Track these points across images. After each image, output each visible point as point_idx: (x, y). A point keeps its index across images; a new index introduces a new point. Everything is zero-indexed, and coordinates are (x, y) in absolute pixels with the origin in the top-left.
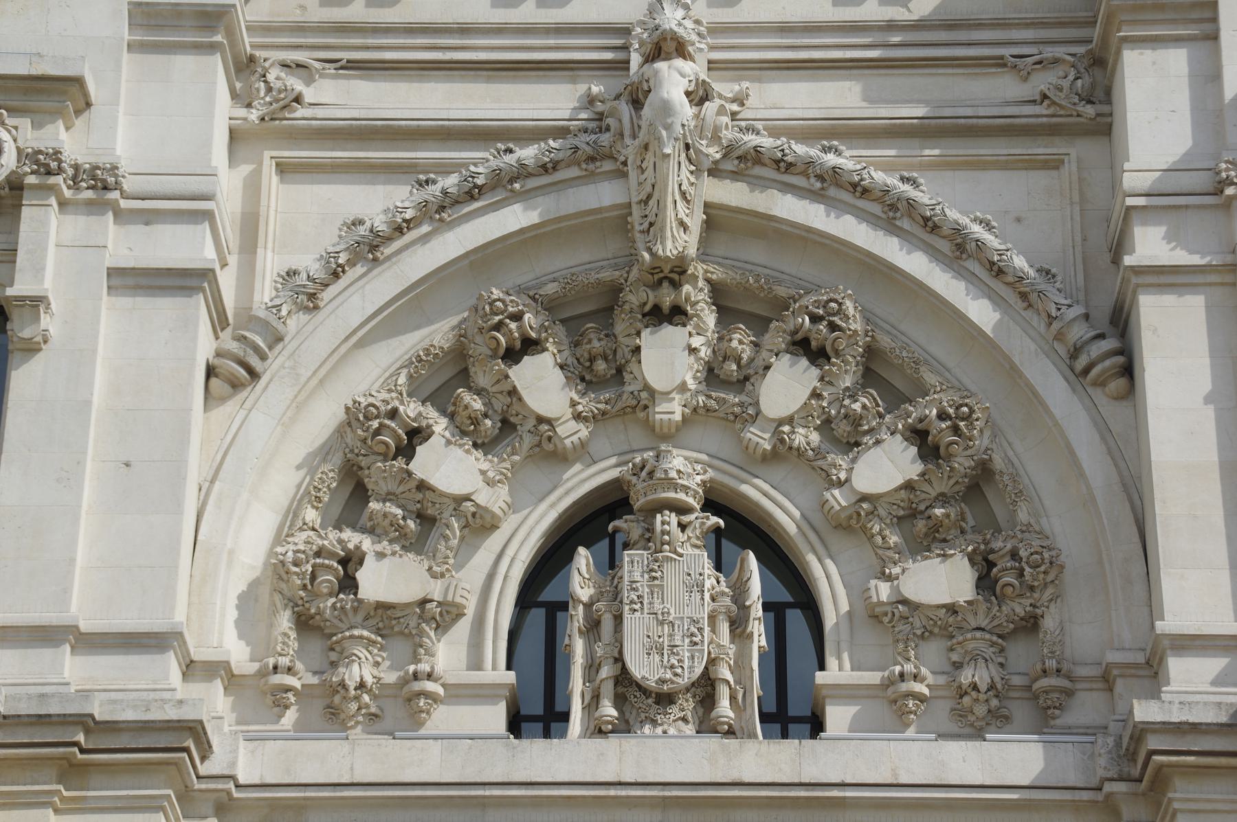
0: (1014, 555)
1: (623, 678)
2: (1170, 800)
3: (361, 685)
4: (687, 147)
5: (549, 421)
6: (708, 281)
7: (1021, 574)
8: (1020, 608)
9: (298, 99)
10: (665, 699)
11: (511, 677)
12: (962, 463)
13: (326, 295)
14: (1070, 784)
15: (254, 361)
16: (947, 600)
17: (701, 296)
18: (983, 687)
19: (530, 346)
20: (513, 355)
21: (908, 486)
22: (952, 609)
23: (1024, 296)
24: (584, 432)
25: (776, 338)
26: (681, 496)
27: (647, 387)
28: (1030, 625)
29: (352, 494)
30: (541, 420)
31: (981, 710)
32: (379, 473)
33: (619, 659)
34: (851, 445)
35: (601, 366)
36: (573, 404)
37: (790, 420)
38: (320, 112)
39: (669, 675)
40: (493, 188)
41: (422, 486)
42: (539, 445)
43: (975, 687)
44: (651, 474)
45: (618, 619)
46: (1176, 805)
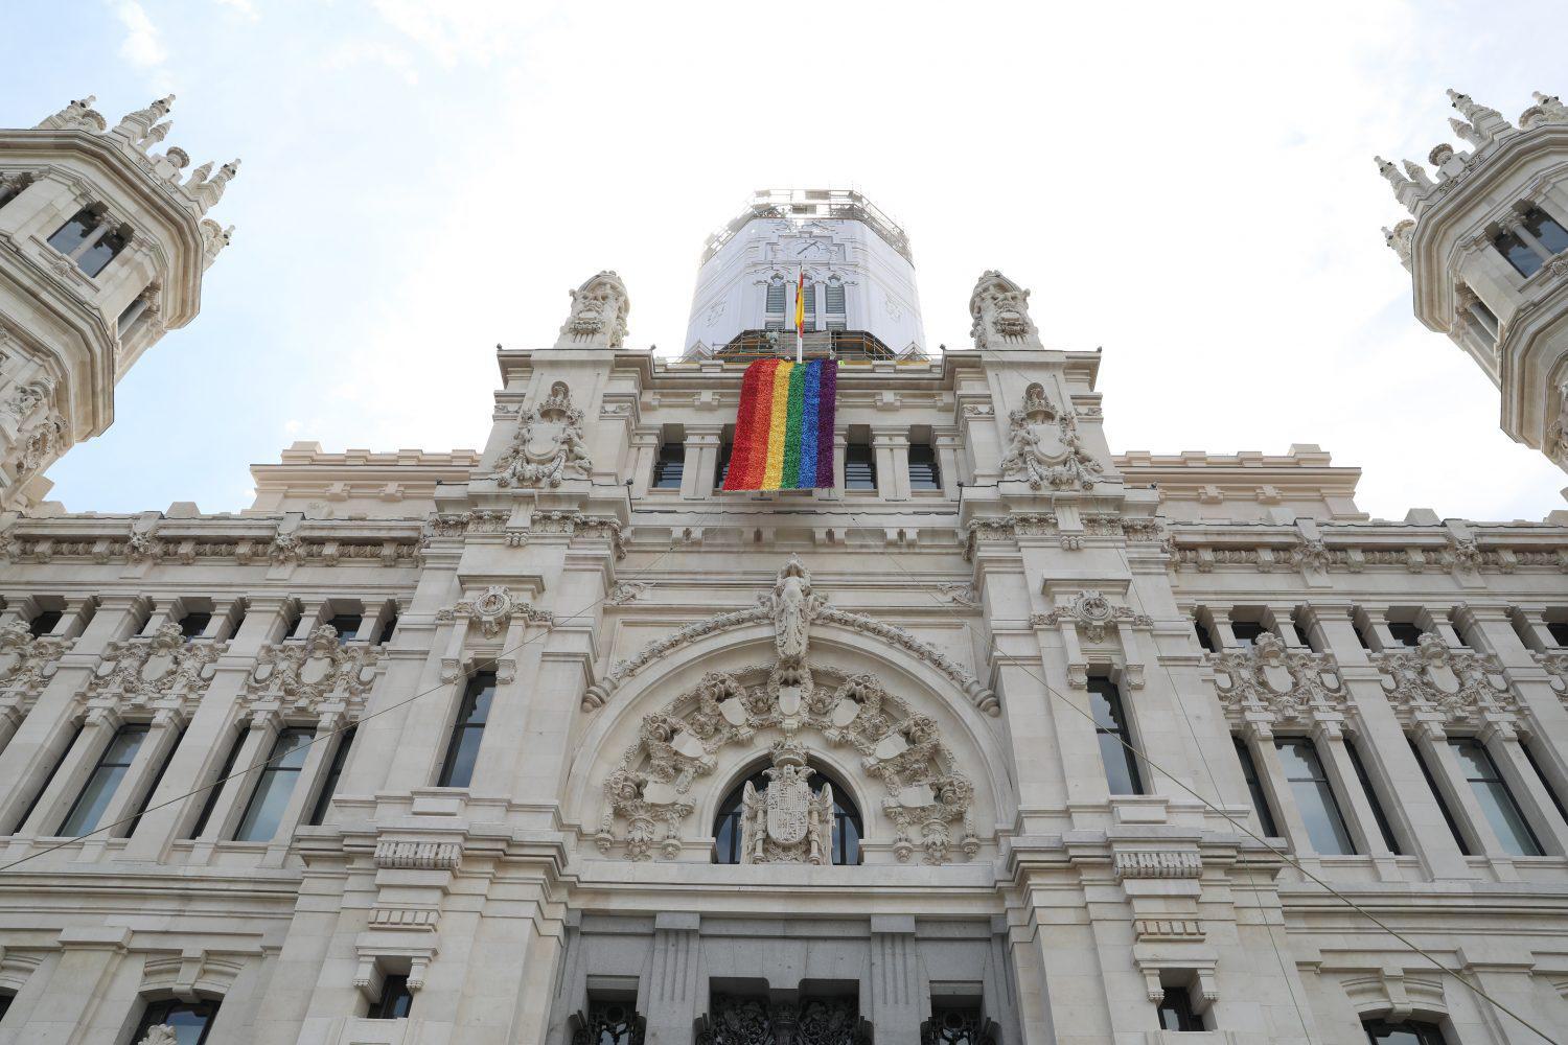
0: (951, 784)
1: (767, 839)
2: (1029, 885)
3: (642, 840)
4: (801, 610)
5: (736, 727)
6: (811, 669)
7: (954, 793)
8: (955, 808)
9: (633, 596)
10: (786, 848)
11: (714, 839)
12: (926, 745)
13: (638, 671)
14: (980, 885)
15: (603, 695)
16: (919, 804)
17: (806, 675)
18: (939, 844)
19: (728, 695)
20: (720, 700)
21: (902, 756)
22: (923, 809)
23: (951, 674)
24: (752, 732)
25: (840, 693)
26: (797, 758)
27: (782, 713)
28: (959, 818)
29: (645, 759)
30: (732, 726)
31: (938, 854)
32: (657, 747)
33: (765, 830)
34: (874, 739)
35: (761, 704)
36: (747, 720)
37: (847, 728)
38: (643, 602)
39: (789, 837)
40: (715, 629)
41: (676, 753)
42: (731, 738)
43: (934, 844)
44: (783, 747)
45: (765, 812)
46: (1032, 887)
